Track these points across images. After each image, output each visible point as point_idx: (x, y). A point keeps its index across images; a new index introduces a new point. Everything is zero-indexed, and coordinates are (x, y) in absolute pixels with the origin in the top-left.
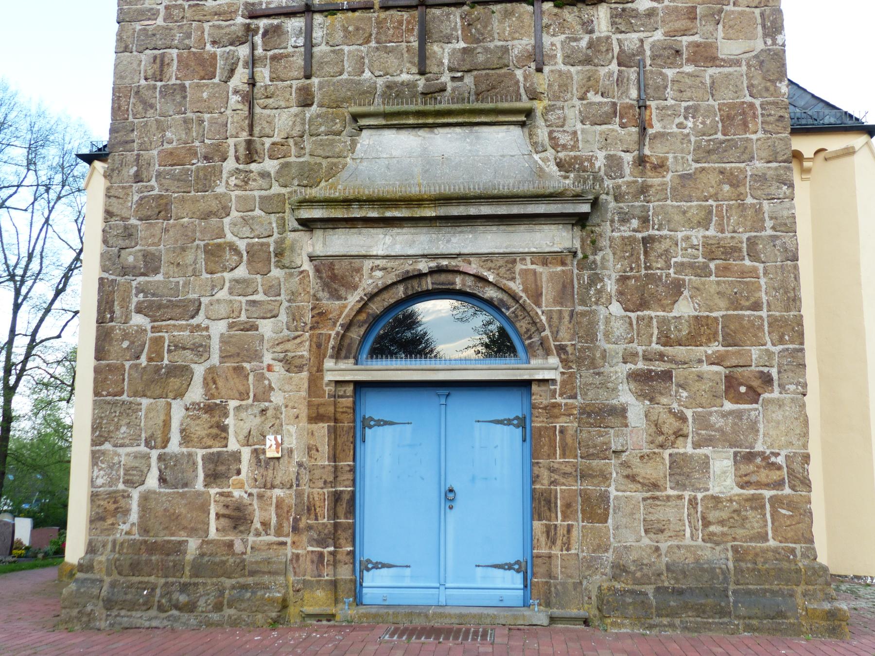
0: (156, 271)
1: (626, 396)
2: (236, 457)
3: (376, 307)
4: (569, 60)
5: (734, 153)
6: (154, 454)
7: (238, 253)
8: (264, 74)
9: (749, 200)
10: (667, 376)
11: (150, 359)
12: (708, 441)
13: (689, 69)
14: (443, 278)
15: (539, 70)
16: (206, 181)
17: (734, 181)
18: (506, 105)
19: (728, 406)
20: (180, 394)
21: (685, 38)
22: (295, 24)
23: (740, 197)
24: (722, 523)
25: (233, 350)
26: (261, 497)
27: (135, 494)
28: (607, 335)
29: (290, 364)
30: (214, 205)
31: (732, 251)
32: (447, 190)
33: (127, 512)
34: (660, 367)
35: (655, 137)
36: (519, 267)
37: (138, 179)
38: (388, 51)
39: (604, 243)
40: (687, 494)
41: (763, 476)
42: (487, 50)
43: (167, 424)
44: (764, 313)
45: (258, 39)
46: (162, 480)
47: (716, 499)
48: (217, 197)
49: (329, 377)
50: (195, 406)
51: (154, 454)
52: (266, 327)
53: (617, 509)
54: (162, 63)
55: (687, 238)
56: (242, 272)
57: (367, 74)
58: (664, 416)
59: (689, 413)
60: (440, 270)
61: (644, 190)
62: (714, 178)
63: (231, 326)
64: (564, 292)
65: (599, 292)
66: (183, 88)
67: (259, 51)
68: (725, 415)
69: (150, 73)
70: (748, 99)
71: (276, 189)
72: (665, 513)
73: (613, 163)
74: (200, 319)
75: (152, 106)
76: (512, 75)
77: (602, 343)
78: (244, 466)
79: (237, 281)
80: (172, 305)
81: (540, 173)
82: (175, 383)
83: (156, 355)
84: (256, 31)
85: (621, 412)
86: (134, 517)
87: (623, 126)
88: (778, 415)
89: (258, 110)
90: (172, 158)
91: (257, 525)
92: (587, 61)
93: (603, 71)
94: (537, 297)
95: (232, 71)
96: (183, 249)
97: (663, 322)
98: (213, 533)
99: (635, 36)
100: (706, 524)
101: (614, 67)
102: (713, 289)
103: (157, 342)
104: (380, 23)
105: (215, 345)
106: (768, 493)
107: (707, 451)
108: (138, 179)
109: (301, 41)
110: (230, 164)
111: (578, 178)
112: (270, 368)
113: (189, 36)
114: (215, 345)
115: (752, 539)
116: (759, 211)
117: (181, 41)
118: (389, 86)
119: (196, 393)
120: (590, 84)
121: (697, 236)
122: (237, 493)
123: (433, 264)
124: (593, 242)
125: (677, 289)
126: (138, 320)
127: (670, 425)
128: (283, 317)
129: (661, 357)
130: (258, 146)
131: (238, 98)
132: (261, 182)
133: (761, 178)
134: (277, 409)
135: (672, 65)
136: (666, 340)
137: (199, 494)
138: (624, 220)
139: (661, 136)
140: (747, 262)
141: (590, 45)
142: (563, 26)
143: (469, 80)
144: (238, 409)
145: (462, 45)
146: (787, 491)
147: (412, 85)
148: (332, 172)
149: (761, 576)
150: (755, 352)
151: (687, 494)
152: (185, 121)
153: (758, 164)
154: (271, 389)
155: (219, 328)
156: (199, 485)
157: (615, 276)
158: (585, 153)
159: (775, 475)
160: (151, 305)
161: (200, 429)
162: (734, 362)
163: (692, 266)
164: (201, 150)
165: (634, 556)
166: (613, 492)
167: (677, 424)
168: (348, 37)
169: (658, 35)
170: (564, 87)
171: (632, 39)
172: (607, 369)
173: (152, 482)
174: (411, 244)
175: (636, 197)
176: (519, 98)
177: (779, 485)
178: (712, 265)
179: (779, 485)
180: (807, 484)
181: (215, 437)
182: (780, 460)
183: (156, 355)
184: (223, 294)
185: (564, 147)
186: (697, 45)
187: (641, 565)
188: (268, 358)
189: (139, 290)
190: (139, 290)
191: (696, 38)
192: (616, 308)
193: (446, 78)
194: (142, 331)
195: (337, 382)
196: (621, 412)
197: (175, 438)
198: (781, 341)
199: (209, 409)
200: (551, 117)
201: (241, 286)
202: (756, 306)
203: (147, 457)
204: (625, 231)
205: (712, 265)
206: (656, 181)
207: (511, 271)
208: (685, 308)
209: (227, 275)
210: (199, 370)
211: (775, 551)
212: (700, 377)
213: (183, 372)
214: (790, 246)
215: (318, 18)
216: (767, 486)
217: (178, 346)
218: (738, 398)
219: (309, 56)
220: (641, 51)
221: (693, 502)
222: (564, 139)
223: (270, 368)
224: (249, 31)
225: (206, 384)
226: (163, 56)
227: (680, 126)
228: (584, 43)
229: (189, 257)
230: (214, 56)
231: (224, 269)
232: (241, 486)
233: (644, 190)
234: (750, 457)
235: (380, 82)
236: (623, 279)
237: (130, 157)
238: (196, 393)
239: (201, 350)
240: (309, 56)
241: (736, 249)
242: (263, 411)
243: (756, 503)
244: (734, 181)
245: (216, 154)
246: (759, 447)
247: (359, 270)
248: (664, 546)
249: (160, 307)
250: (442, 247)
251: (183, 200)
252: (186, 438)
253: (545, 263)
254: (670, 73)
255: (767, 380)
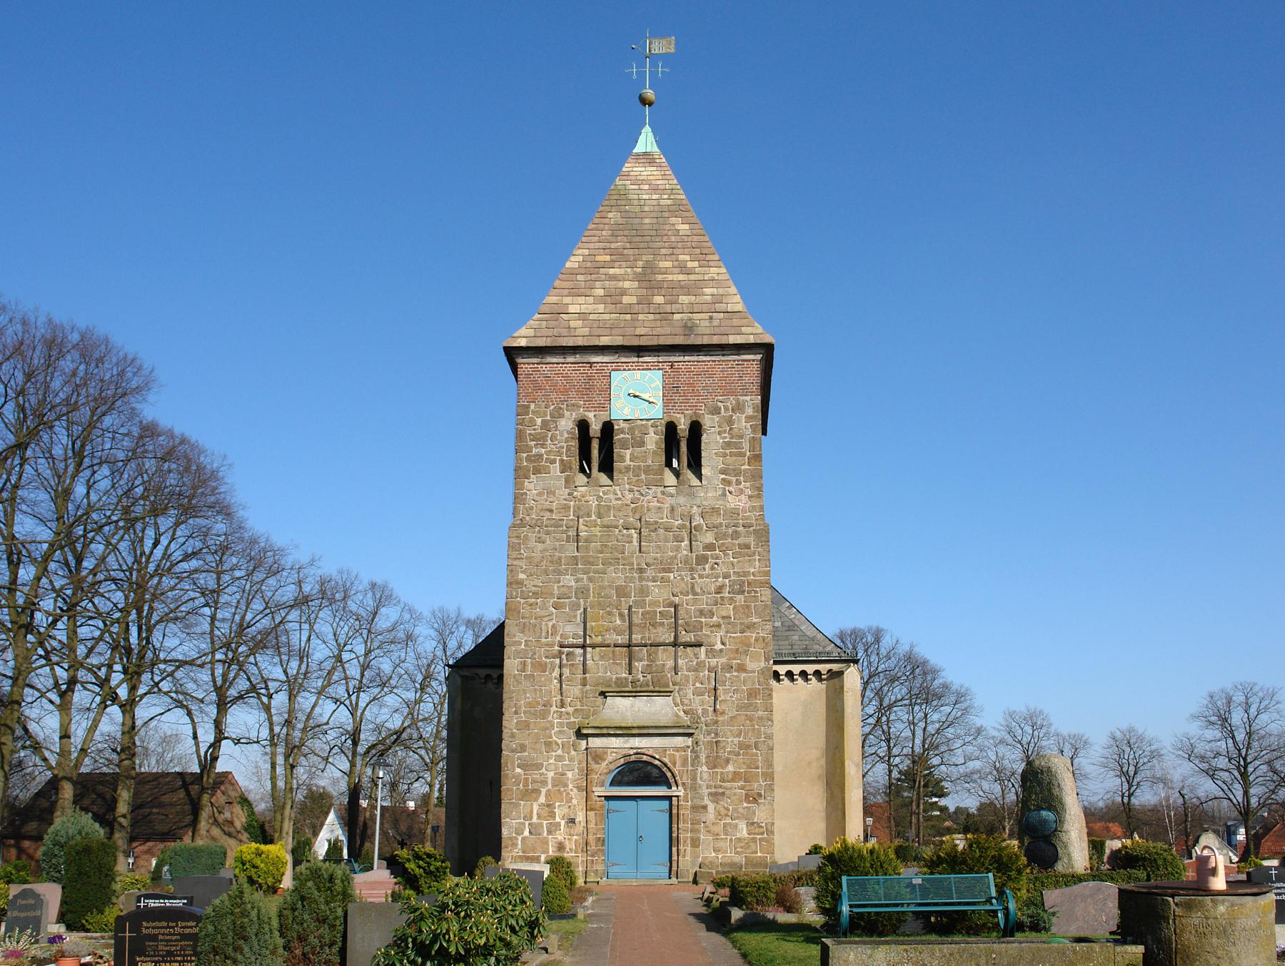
0: (525, 751)
1: (706, 801)
2: (559, 824)
3: (612, 767)
4: (689, 670)
5: (752, 708)
6: (527, 823)
7: (558, 745)
8: (566, 671)
9: (756, 727)
10: (723, 794)
11: (524, 786)
12: (738, 818)
13: (735, 674)
14: (638, 756)
15: (676, 674)
16: (544, 714)
17: (750, 719)
18: (662, 690)
19: (745, 805)
20: (536, 800)
21: (735, 661)
22: (580, 651)
23: (753, 725)
24: (741, 848)
25: (557, 783)
26: (569, 839)
27: (520, 838)
28: (701, 778)
29: (579, 788)
30: (549, 725)
31: (748, 747)
32: (641, 724)
33: (517, 845)
34: (721, 790)
35: (721, 702)
36: (668, 752)
37: (516, 713)
38: (617, 664)
39: (701, 743)
40: (729, 837)
41: (757, 830)
42: (656, 665)
43: (532, 811)
44: (760, 770)
45: (564, 656)
46: (530, 832)
47: (739, 839)
48: (549, 722)
49: (596, 794)
50: (542, 805)
51: (527, 823)
52: (569, 774)
53: (703, 842)
54: (524, 664)
55: (732, 741)
56: (560, 752)
57: (609, 674)
58: (722, 809)
59: (731, 808)
60: (637, 754)
61: (716, 722)
62: (743, 718)
63: (555, 774)
64: (685, 763)
65: (698, 762)
66: (533, 675)
67: (565, 662)
68: (744, 808)
69: (519, 668)
70: (758, 686)
71: (572, 719)
72: (721, 844)
73: (705, 712)
74: (544, 769)
75: (521, 683)
76: (666, 676)
77: (699, 781)
78: (562, 828)
79: (559, 756)
80: (532, 765)
81: (677, 716)
82: (534, 795)
83: (526, 784)
84: (563, 653)
85: (705, 807)
86: (520, 846)
87: (709, 696)
88: (764, 808)
89: (564, 686)
90: (530, 705)
91: (568, 849)
92: (696, 670)
93: (701, 674)
94: (674, 764)
95: (554, 670)
96: (536, 743)
97: (722, 773)
98: (551, 853)
99: (715, 660)
100: (735, 848)
101: (706, 672)
102: (741, 761)
103: (527, 779)
104: (613, 652)
105: (550, 781)
106: (759, 837)
107: (737, 821)
108: (516, 713)
109: (582, 659)
110: (554, 708)
111: (691, 718)
112: (571, 790)
113: (535, 654)
114: (550, 781)
115: (752, 853)
116: (759, 730)
117: (532, 655)
118: (617, 678)
119: (542, 799)
120: (697, 679)
121: (736, 740)
122: (559, 838)
123: (635, 751)
124: (697, 743)
125: (728, 761)
126: (518, 770)
127: (723, 812)
128: (576, 770)
129: (721, 787)
130: (565, 702)
131: (556, 681)
132: (567, 716)
133: (761, 718)
134: (575, 806)
135: (729, 672)
136: (723, 780)
137: (545, 838)
138: (709, 734)
139: (725, 701)
140: (754, 751)
141: (697, 664)
142: (687, 656)
143: (649, 677)
144: (559, 806)
145: (646, 663)
146: (765, 835)
147: (626, 679)
148: (595, 713)
149: (754, 865)
150: (756, 785)
151: (729, 837)
152: (535, 690)
153: (760, 712)
154: (572, 798)
155: (551, 774)
156: (545, 834)
157: (704, 756)
158: (694, 708)
159: (761, 830)
160: (523, 765)
161: (545, 812)
162: (748, 788)
163: (734, 752)
164: (542, 703)
165: (709, 860)
166: (702, 837)
167: (726, 812)
168: (602, 658)
169: (724, 660)
170: (688, 681)
171: (713, 662)
172: (700, 791)
173: (526, 833)
174: (626, 742)
175: (714, 725)
176: (668, 686)
177: (762, 834)
178: (741, 752)
179: (762, 834)
180: (772, 833)
181: (550, 816)
182: (763, 825)
183: (526, 784)
184: (552, 761)
185: (687, 705)
186: (739, 664)
187: (711, 862)
188: (570, 786)
189: (518, 759)
190: (518, 759)
191: (739, 661)
192: (705, 768)
193: (640, 676)
194: (519, 774)
195: (599, 796)
196: (705, 807)
197: (535, 817)
198: (766, 780)
199: (548, 806)
200: (681, 693)
201: (559, 758)
202: (757, 768)
203: (524, 824)
204: (708, 738)
205: (741, 752)
206: (721, 718)
207: (665, 754)
208: (730, 768)
209: (554, 754)
210: (544, 791)
211: (760, 857)
212: (735, 794)
213: (538, 792)
214: (771, 745)
215: (589, 649)
216: (758, 834)
217: (534, 781)
218: (749, 802)
219: (584, 664)
220: (717, 666)
221: (731, 840)
222: (686, 702)
223: (571, 790)
224: (561, 653)
225: (546, 797)
226: (525, 661)
227: (731, 697)
228: (695, 663)
229: (538, 746)
230: (546, 663)
231: (553, 751)
232: (560, 834)
233: (716, 722)
234: (753, 824)
235: (614, 676)
236: (708, 757)
237: (513, 704)
238: (542, 799)
239: (544, 783)
240: (584, 664)
241: (750, 746)
242: (570, 807)
243: (754, 840)
244: (750, 719)
245: (547, 704)
246: (756, 820)
247: (606, 753)
248: (720, 856)
249: (527, 766)
250: (637, 745)
251: (535, 723)
252: (539, 816)
253: (678, 751)
254: (728, 675)
255: (760, 795)
